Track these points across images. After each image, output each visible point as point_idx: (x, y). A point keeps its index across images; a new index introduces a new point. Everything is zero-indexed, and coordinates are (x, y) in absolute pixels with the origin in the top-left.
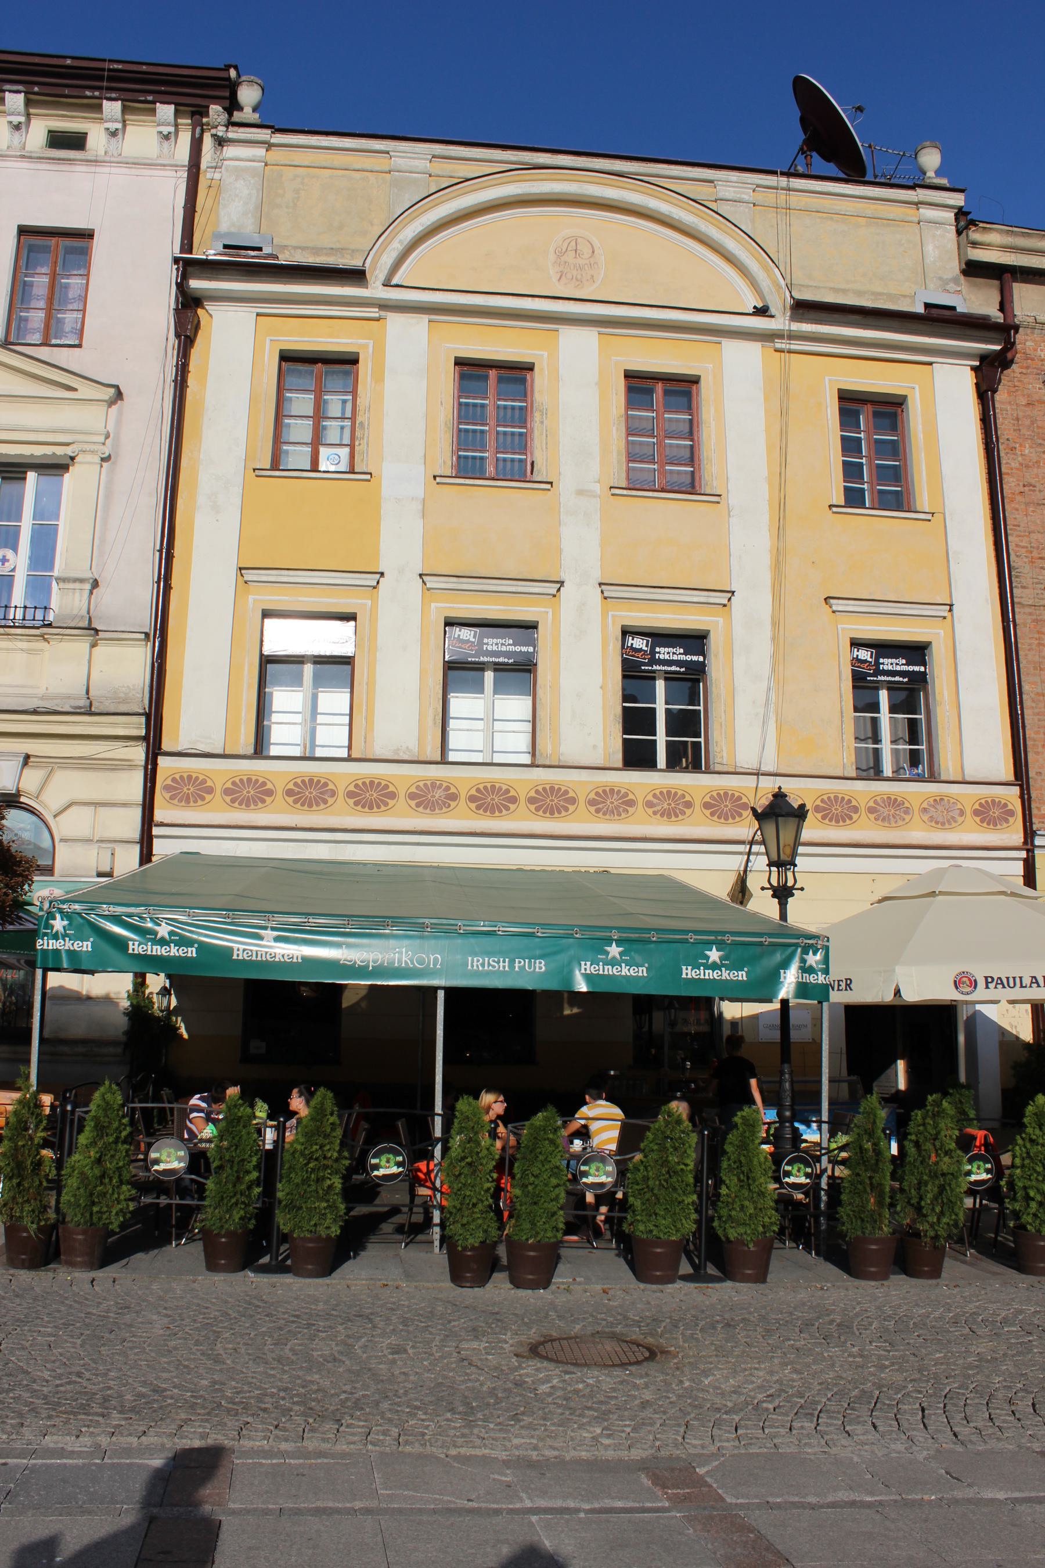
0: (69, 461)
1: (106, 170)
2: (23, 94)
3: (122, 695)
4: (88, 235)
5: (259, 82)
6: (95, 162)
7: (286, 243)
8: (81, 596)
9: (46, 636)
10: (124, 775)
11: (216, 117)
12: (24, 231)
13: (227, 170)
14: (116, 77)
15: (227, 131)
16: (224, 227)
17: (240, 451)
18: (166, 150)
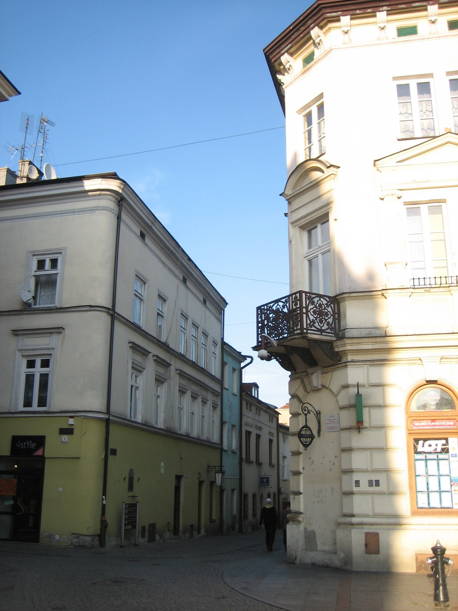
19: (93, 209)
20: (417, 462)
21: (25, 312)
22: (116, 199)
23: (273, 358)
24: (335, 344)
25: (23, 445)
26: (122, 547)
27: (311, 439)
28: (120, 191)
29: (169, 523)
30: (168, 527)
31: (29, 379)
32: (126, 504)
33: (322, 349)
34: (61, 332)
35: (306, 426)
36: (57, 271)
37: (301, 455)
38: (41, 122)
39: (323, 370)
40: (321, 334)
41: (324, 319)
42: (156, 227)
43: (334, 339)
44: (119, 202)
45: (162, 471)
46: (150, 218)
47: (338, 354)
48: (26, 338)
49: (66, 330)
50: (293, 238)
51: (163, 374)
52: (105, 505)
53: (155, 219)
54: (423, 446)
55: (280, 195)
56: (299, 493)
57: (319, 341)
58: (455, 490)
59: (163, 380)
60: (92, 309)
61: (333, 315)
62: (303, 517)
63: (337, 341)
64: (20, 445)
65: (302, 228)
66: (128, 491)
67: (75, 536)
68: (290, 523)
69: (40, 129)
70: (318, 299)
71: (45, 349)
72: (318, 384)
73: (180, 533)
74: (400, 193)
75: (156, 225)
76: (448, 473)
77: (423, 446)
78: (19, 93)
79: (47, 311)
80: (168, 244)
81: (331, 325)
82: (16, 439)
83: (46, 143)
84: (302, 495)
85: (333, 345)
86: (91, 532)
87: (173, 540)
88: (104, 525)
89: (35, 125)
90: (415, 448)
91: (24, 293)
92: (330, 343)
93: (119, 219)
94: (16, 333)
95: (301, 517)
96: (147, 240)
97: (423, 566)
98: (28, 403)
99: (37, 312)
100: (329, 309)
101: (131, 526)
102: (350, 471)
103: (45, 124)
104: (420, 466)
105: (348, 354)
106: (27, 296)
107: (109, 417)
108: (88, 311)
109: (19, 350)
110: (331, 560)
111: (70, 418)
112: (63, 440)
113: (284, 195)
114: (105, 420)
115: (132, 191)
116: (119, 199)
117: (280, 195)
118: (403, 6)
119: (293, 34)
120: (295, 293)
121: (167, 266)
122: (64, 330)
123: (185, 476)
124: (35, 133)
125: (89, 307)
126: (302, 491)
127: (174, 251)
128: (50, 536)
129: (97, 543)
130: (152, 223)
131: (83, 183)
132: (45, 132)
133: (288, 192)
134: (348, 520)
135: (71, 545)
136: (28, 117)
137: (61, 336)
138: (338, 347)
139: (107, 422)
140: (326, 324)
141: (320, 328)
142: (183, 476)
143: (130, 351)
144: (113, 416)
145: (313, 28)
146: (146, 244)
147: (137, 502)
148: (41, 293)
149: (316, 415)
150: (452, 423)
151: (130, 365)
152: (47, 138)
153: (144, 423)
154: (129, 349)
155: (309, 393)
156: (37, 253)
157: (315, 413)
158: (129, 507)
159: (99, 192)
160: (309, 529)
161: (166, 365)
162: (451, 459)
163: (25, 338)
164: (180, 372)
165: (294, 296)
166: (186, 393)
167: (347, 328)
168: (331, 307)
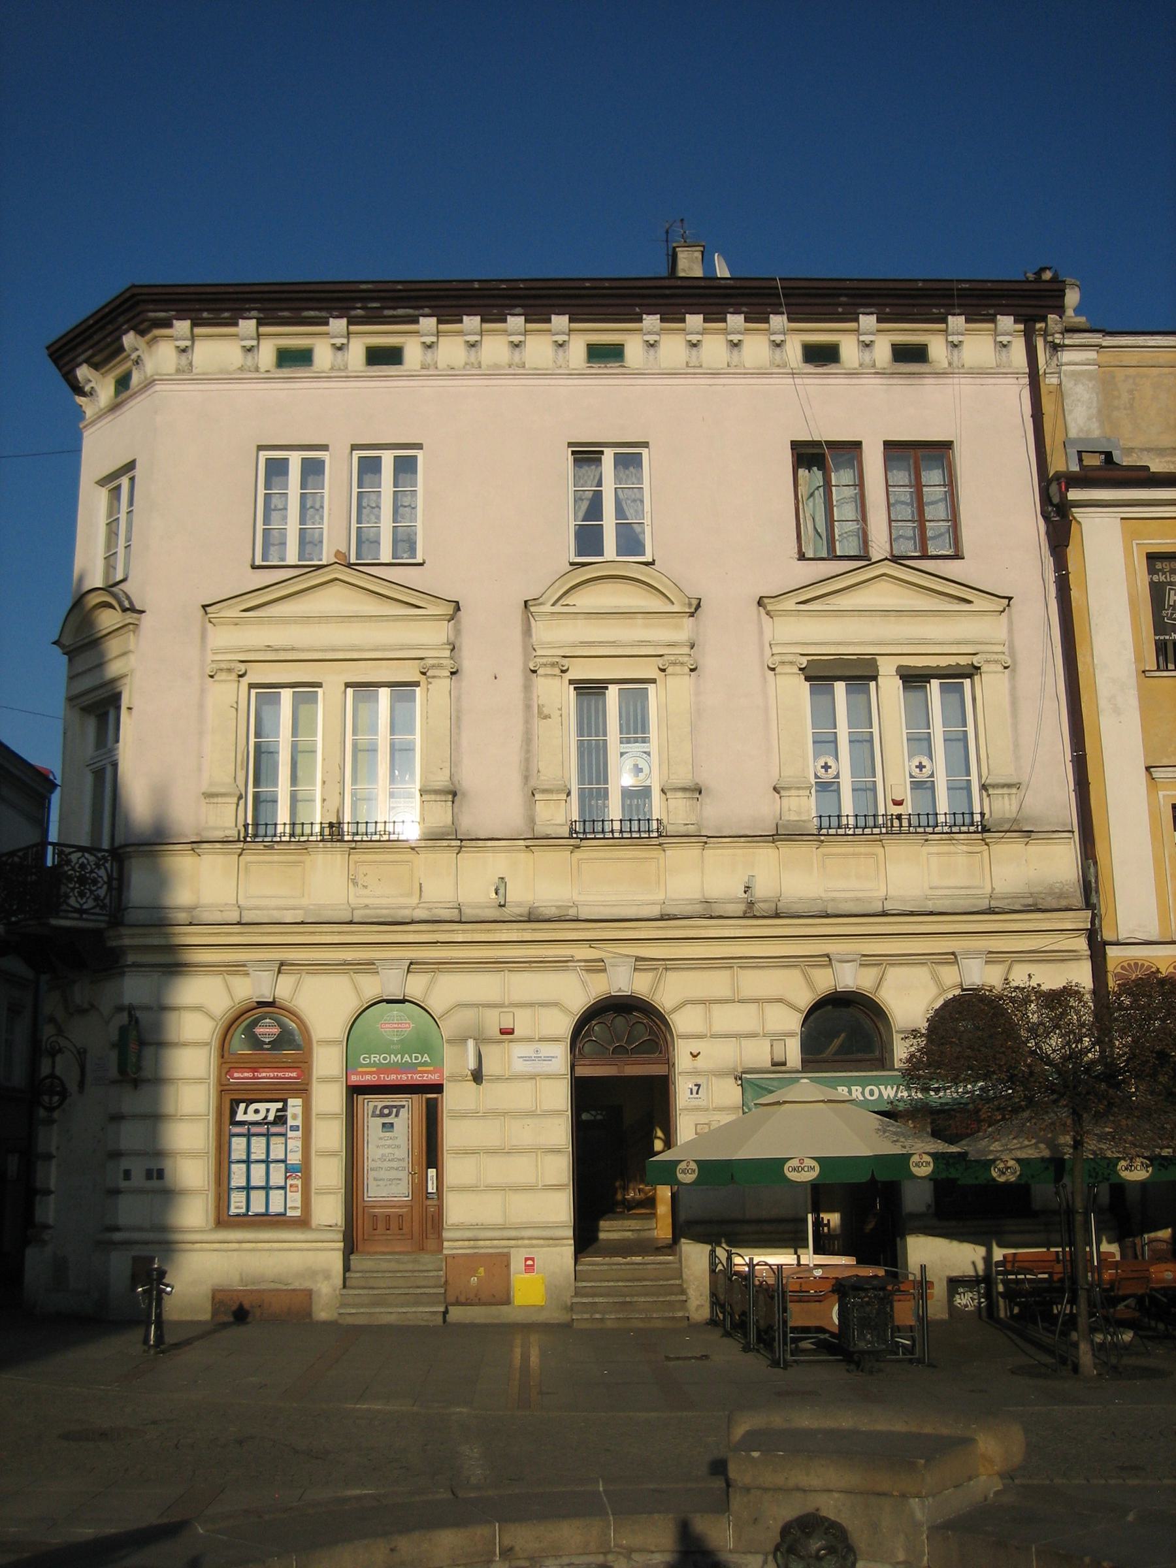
0: (973, 671)
1: (956, 381)
2: (875, 316)
3: (1057, 890)
4: (948, 445)
5: (1078, 283)
6: (943, 374)
7: (1130, 445)
8: (1010, 799)
9: (987, 840)
10: (1073, 964)
11: (1053, 326)
12: (888, 445)
13: (1065, 376)
14: (964, 294)
15: (1064, 338)
16: (1073, 433)
17: (1129, 654)
18: (1004, 358)
20: (234, 1140)
35: (52, 1076)
40: (80, 919)
41: (90, 890)
43: (103, 925)
54: (245, 1113)
55: (54, 643)
56: (48, 1192)
58: (291, 1186)
61: (109, 883)
70: (80, 854)
74: (243, 667)
76: (282, 1157)
77: (245, 1113)
81: (102, 901)
84: (52, 1196)
90: (233, 1113)
92: (98, 934)
97: (223, 1309)
100: (102, 872)
102: (116, 1155)
104: (238, 1146)
117: (54, 643)
118: (286, 314)
119: (95, 333)
126: (53, 1189)
133: (66, 641)
134: (108, 1235)
145: (126, 332)
149: (78, 1056)
150: (294, 1075)
157: (75, 1053)
162: (290, 1134)
167: (130, 906)
168: (106, 869)
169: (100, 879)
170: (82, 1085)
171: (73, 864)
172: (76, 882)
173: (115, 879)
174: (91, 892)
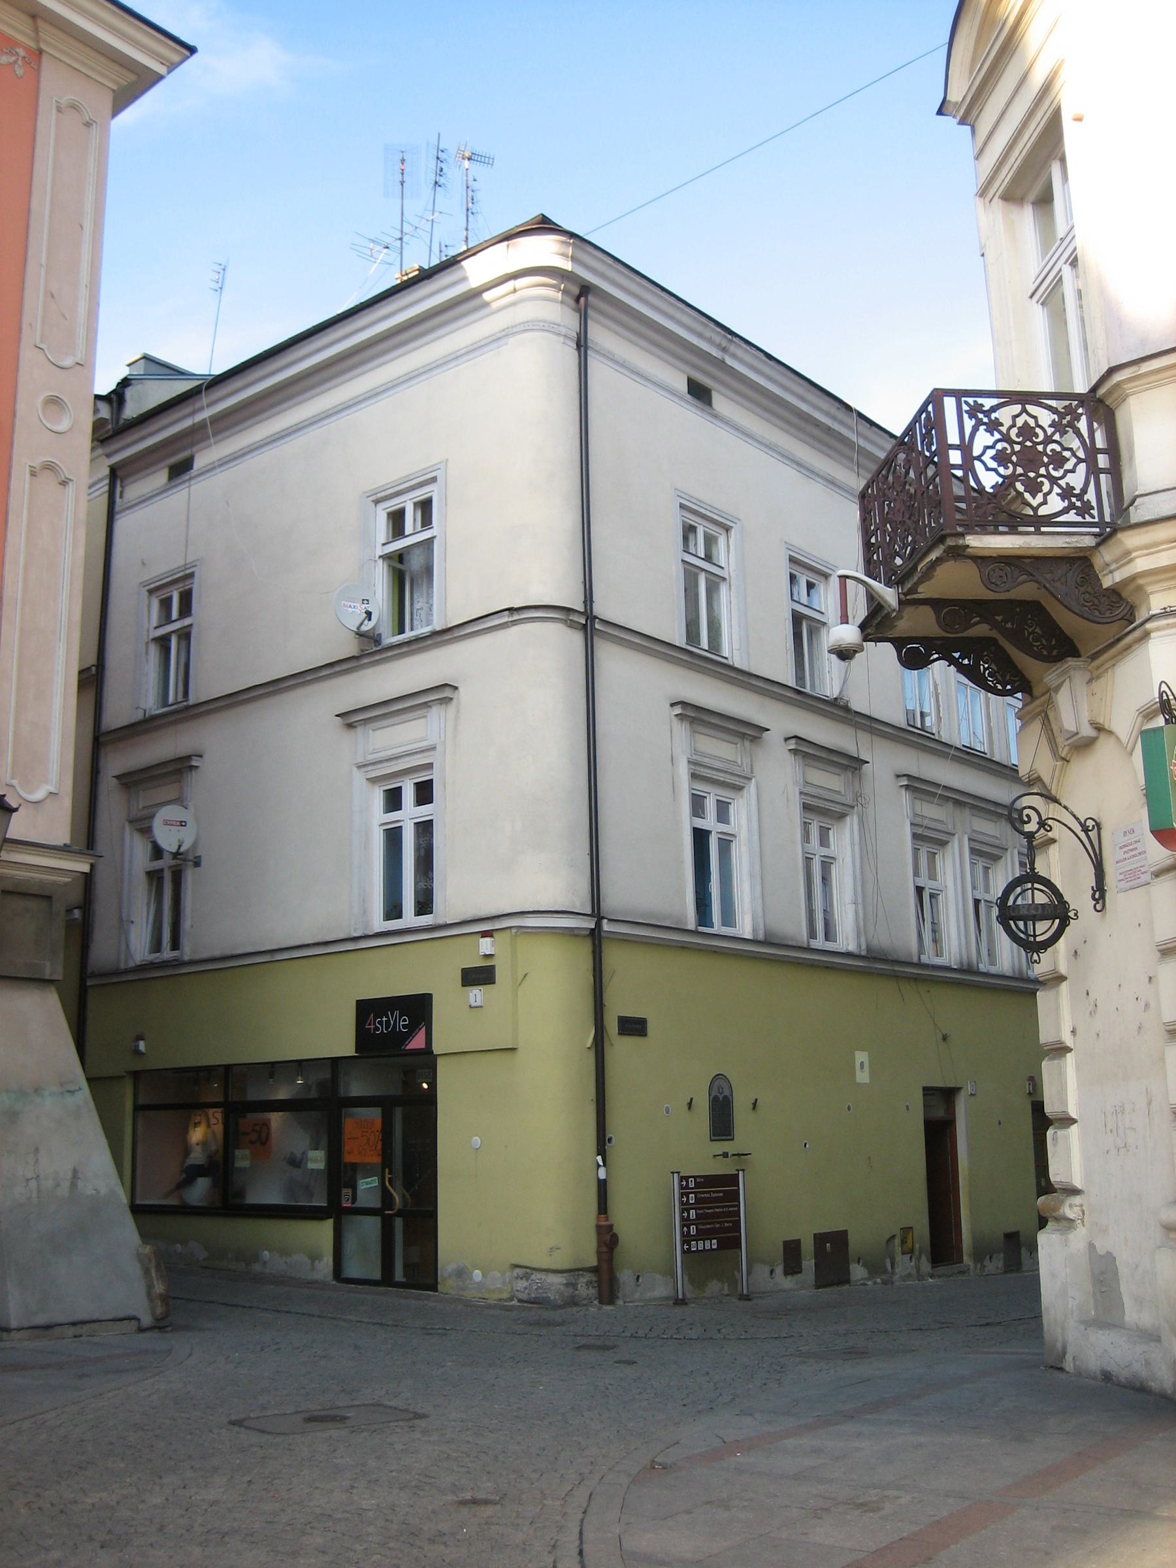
19: (499, 335)
21: (366, 661)
22: (565, 292)
23: (936, 656)
24: (1098, 561)
25: (381, 1023)
26: (680, 1302)
27: (1057, 921)
28: (568, 265)
29: (906, 1230)
30: (903, 1242)
31: (393, 837)
32: (682, 1179)
33: (1044, 586)
34: (451, 699)
36: (431, 530)
37: (1064, 986)
38: (438, 158)
39: (1089, 668)
40: (1038, 532)
42: (741, 361)
43: (1089, 541)
44: (577, 300)
45: (863, 1077)
46: (708, 334)
47: (1119, 595)
48: (373, 730)
49: (460, 689)
50: (987, 245)
51: (838, 792)
52: (605, 1181)
53: (730, 337)
55: (940, 112)
56: (1069, 1121)
57: (1027, 561)
59: (838, 808)
60: (516, 617)
62: (1081, 1206)
63: (1101, 548)
64: (374, 1024)
65: (1012, 196)
66: (711, 1140)
67: (518, 1270)
68: (1050, 1225)
69: (438, 177)
70: (1017, 408)
71: (416, 753)
72: (1078, 723)
73: (965, 1258)
75: (740, 353)
78: (192, 50)
79: (414, 647)
80: (804, 407)
81: (1080, 497)
82: (367, 1009)
83: (472, 213)
85: (1091, 566)
86: (561, 1260)
87: (931, 1280)
88: (608, 1240)
89: (423, 170)
91: (350, 606)
93: (582, 349)
94: (352, 719)
95: (1071, 1206)
96: (720, 402)
98: (393, 910)
99: (390, 654)
101: (714, 1241)
103: (466, 163)
105: (1149, 589)
106: (353, 617)
107: (598, 924)
108: (508, 627)
109: (360, 767)
110: (1148, 1363)
111: (483, 937)
112: (473, 1004)
113: (951, 108)
114: (588, 935)
115: (610, 261)
116: (576, 290)
117: (940, 112)
120: (924, 409)
121: (818, 475)
122: (457, 691)
123: (969, 1088)
124: (427, 191)
125: (507, 613)
126: (1074, 1115)
127: (836, 426)
128: (461, 1273)
129: (585, 1289)
130: (724, 350)
131: (462, 267)
132: (468, 187)
133: (955, 96)
135: (511, 1299)
136: (401, 154)
137: (452, 707)
138: (1111, 572)
139: (595, 937)
140: (1058, 494)
141: (1032, 513)
142: (959, 1089)
143: (681, 731)
144: (610, 920)
146: (716, 416)
147: (738, 1170)
148: (415, 601)
149: (1082, 835)
151: (683, 771)
152: (475, 200)
153: (761, 937)
154: (675, 721)
155: (1068, 761)
156: (382, 494)
157: (1078, 829)
158: (697, 1185)
159: (510, 285)
160: (1102, 1246)
161: (852, 764)
163: (371, 731)
164: (908, 780)
165: (924, 416)
166: (950, 844)
167: (1137, 493)
169: (1067, 454)
170: (1099, 892)
171: (1004, 429)
172: (1015, 465)
173: (1101, 451)
174: (1054, 481)
